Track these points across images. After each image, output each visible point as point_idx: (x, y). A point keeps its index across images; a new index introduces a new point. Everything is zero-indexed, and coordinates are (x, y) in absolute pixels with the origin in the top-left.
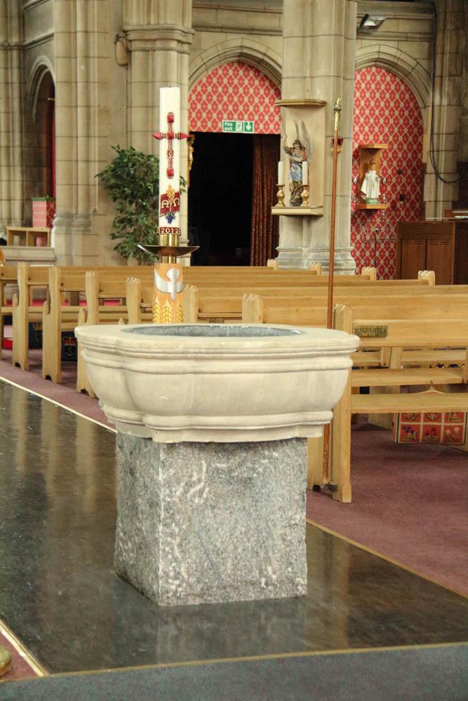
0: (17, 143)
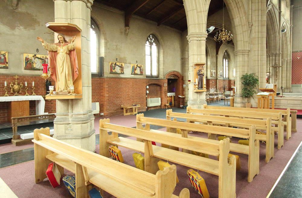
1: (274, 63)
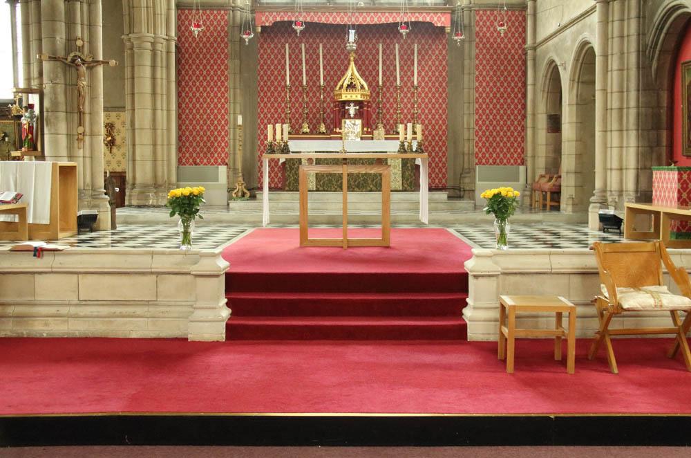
0: (633, 103)
1: (61, 38)
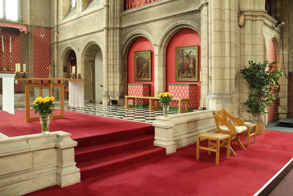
0: (118, 63)
